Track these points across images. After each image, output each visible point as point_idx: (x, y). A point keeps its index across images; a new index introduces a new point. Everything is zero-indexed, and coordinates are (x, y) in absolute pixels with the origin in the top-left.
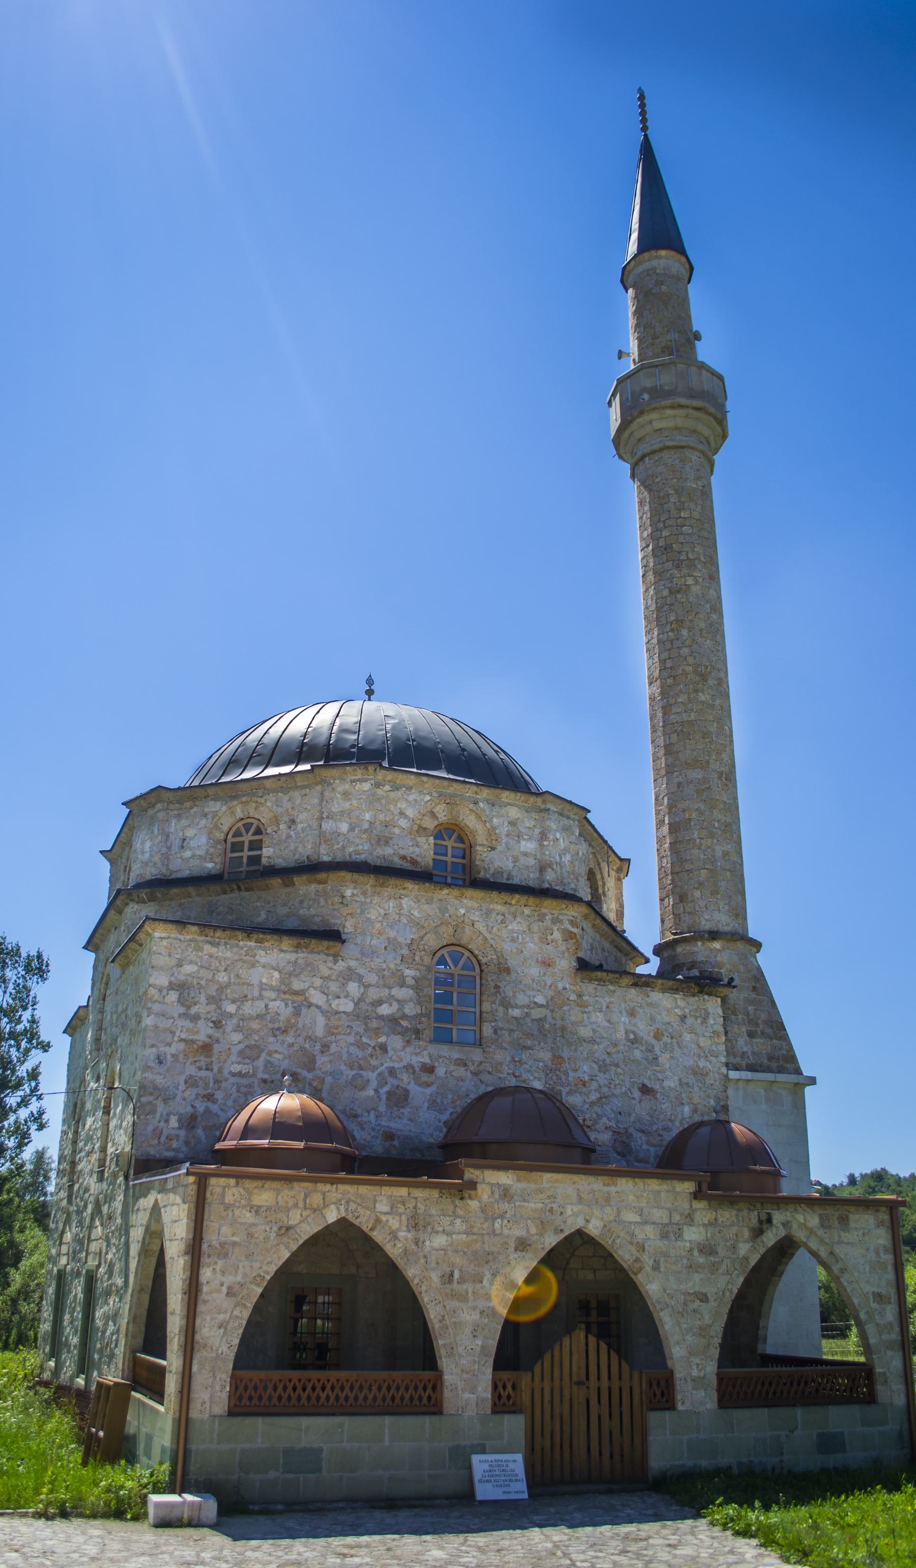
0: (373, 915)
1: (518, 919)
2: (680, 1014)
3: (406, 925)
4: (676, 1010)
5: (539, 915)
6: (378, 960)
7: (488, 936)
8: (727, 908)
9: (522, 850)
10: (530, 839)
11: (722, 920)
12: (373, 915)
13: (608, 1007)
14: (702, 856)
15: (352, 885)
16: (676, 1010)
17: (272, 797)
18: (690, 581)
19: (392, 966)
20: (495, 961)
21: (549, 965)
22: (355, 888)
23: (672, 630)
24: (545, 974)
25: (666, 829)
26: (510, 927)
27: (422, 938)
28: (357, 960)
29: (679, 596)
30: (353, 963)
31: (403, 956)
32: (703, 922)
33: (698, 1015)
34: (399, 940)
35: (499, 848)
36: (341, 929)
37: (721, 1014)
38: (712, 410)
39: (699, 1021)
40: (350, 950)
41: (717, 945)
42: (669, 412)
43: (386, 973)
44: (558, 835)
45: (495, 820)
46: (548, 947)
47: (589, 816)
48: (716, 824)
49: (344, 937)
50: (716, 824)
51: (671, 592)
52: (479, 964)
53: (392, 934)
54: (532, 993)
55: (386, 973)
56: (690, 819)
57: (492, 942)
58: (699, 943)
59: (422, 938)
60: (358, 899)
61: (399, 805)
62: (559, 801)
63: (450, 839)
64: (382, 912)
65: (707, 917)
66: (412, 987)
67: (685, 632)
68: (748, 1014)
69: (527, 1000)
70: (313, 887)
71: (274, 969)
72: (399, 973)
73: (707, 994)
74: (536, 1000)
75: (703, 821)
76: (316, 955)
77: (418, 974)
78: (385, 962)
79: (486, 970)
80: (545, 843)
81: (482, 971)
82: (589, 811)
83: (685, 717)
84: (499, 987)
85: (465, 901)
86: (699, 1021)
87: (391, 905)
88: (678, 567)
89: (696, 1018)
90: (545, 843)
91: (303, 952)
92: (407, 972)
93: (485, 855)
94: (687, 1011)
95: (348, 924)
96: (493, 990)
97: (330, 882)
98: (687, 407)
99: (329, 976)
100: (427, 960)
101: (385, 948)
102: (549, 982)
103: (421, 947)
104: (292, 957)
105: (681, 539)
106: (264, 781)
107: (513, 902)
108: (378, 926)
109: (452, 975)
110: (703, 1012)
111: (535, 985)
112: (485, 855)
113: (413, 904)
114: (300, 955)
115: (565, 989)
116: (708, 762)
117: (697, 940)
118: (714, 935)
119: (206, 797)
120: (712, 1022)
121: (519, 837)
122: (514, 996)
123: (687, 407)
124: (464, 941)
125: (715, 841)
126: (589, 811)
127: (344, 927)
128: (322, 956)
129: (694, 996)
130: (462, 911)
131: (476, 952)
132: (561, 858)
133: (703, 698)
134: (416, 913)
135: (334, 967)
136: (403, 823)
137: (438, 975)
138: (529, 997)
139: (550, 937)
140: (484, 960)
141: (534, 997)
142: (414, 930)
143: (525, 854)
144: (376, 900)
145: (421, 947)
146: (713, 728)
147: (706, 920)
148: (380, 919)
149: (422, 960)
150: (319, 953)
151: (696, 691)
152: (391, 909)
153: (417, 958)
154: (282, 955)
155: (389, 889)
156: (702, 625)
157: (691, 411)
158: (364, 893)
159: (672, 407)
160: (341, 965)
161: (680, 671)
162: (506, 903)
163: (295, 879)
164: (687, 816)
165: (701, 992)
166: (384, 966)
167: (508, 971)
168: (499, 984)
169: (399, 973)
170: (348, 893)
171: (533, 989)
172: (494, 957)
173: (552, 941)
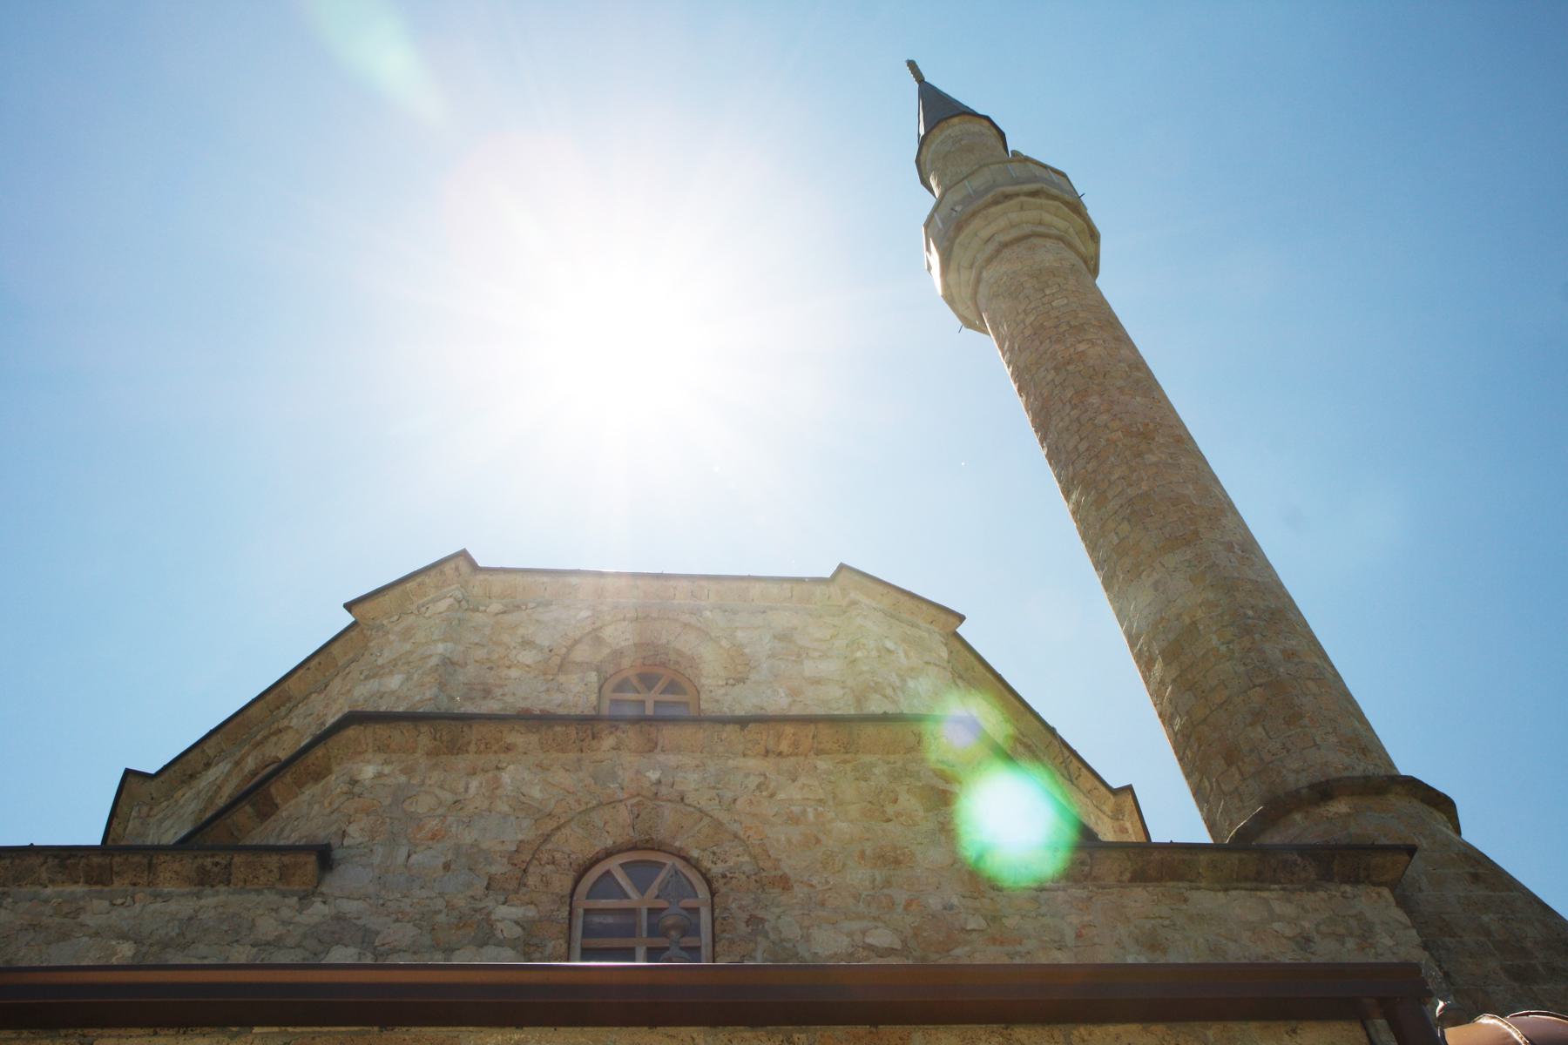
0: (422, 805)
1: (802, 780)
2: (1288, 932)
3: (505, 816)
4: (1276, 926)
5: (855, 769)
6: (424, 893)
7: (724, 817)
8: (1333, 739)
9: (807, 673)
10: (824, 656)
11: (1338, 762)
12: (422, 805)
13: (1079, 936)
14: (1242, 668)
15: (381, 757)
16: (1276, 926)
17: (301, 709)
18: (1082, 347)
19: (461, 903)
20: (747, 868)
21: (897, 862)
22: (386, 762)
23: (1074, 407)
24: (888, 883)
25: (1158, 667)
26: (781, 796)
27: (547, 838)
28: (365, 897)
29: (1070, 368)
30: (351, 907)
31: (491, 878)
32: (1291, 778)
33: (1341, 930)
34: (484, 846)
35: (753, 676)
36: (335, 842)
37: (1404, 919)
38: (1054, 191)
39: (1351, 943)
40: (350, 878)
41: (1340, 807)
42: (993, 210)
43: (442, 918)
44: (889, 645)
45: (740, 634)
46: (890, 826)
47: (962, 630)
48: (1250, 613)
49: (337, 854)
50: (1250, 613)
51: (1057, 369)
52: (709, 882)
53: (468, 837)
54: (856, 925)
55: (442, 918)
56: (1194, 623)
57: (735, 827)
58: (1298, 817)
59: (547, 838)
60: (388, 781)
61: (521, 631)
62: (881, 589)
63: (650, 689)
64: (448, 797)
65: (1295, 766)
66: (512, 943)
67: (1095, 400)
68: (1488, 933)
69: (845, 941)
70: (310, 791)
71: (124, 937)
72: (478, 916)
73: (1346, 880)
74: (869, 940)
75: (1221, 615)
76: (253, 896)
77: (532, 912)
78: (441, 895)
79: (723, 890)
80: (859, 654)
81: (713, 893)
82: (962, 618)
83: (1131, 492)
84: (762, 920)
85: (661, 758)
86: (1351, 943)
87: (474, 784)
88: (1058, 341)
89: (1341, 938)
90: (859, 654)
91: (217, 893)
92: (502, 911)
93: (723, 691)
94: (1306, 924)
95: (352, 829)
96: (743, 929)
97: (336, 769)
98: (1017, 195)
99: (280, 938)
100: (562, 883)
101: (447, 867)
102: (901, 897)
103: (545, 857)
104: (183, 907)
105: (1054, 314)
106: (285, 685)
107: (784, 746)
108: (433, 824)
109: (632, 912)
110: (1353, 923)
111: (862, 907)
112: (723, 691)
113: (527, 775)
114: (209, 901)
115: (949, 907)
116: (1196, 533)
117: (1289, 812)
118: (1324, 791)
119: (208, 765)
120: (1388, 942)
121: (799, 655)
122: (807, 938)
123: (1017, 195)
124: (662, 833)
125: (1257, 636)
126: (962, 618)
127: (344, 834)
128: (271, 897)
129: (1312, 889)
130: (654, 775)
131: (695, 853)
132: (904, 681)
133: (1154, 459)
134: (536, 792)
135: (299, 918)
136: (528, 657)
137: (597, 919)
138: (850, 934)
139: (890, 810)
140: (717, 869)
141: (864, 933)
142: (526, 823)
143: (817, 682)
144: (436, 776)
145: (545, 857)
146: (1190, 490)
147: (1297, 772)
148: (440, 811)
149: (547, 884)
150: (259, 892)
151: (1140, 455)
152: (472, 790)
153: (532, 880)
154: (158, 905)
155: (471, 756)
156: (1120, 383)
157: (1023, 198)
158: (408, 771)
159: (996, 202)
160: (318, 910)
161: (1103, 442)
162: (767, 753)
163: (273, 790)
164: (1187, 621)
165: (1326, 876)
166: (440, 904)
167: (785, 883)
168: (760, 913)
169: (478, 916)
170: (368, 772)
171: (860, 917)
172: (746, 858)
173: (898, 815)
